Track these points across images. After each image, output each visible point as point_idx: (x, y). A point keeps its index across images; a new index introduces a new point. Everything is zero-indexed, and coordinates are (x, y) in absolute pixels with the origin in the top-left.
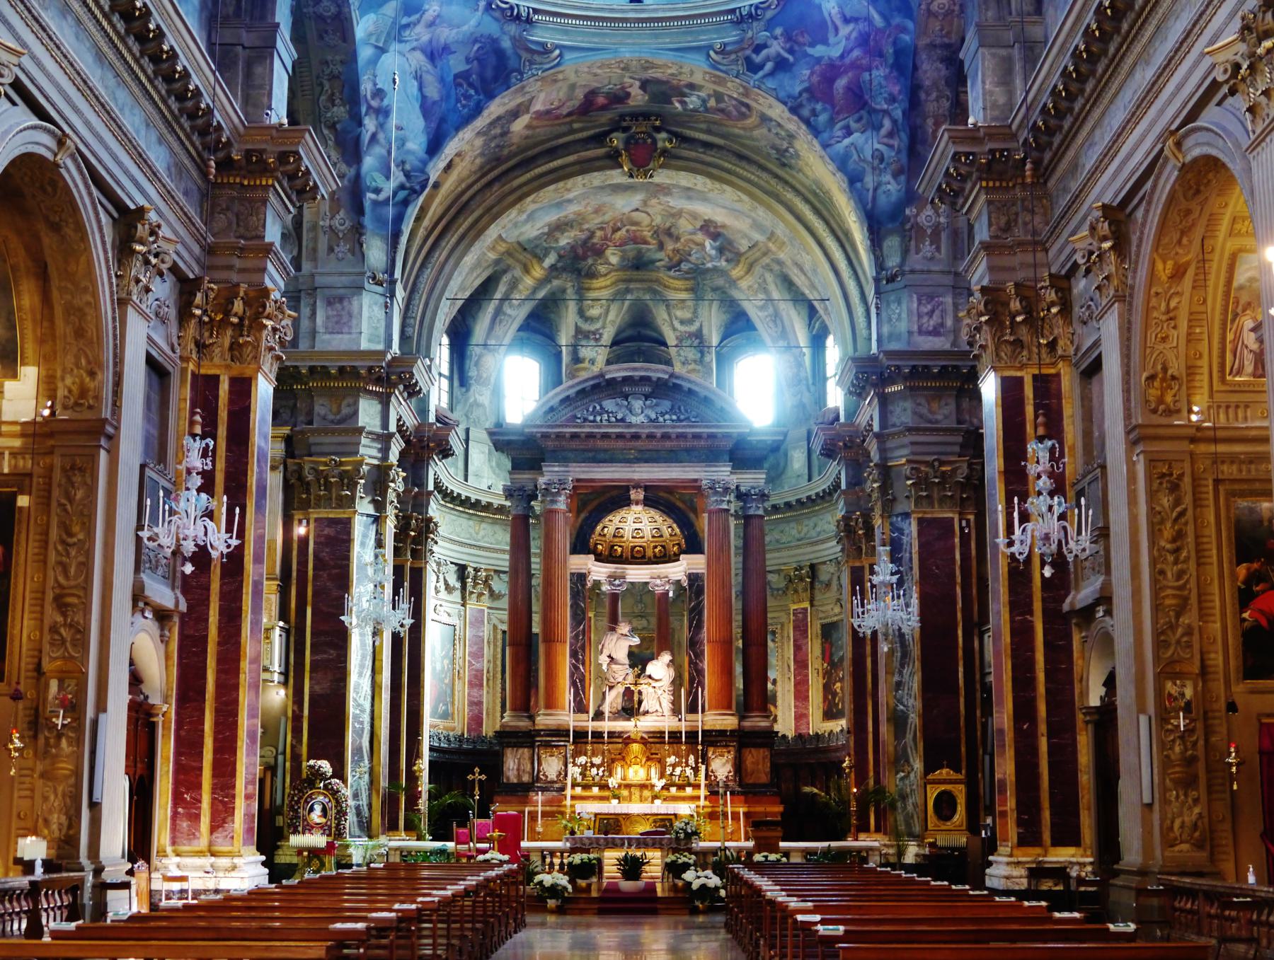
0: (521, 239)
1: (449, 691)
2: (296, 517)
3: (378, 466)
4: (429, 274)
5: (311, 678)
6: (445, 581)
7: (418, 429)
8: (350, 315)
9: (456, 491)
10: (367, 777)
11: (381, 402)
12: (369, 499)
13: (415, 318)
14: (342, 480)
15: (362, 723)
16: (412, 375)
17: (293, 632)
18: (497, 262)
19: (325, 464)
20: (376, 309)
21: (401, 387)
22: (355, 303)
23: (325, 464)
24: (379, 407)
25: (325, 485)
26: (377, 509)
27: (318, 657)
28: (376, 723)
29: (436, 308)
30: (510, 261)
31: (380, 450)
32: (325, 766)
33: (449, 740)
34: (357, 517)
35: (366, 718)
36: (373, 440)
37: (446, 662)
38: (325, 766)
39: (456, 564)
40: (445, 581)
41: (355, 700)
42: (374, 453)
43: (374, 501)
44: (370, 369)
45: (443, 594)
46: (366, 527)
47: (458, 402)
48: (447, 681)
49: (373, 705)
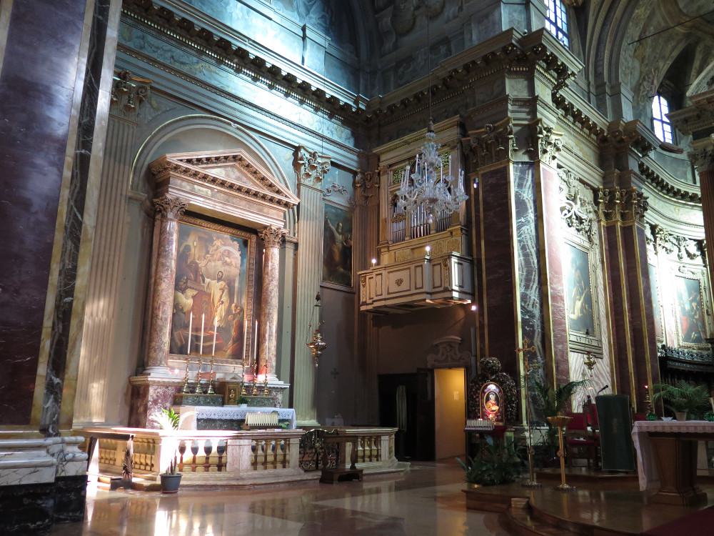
0: (702, 12)
1: (699, 324)
2: (473, 178)
3: (528, 125)
4: (611, 27)
5: (487, 295)
6: (687, 252)
7: (612, 127)
8: (494, 24)
9: (683, 189)
10: (541, 371)
11: (526, 80)
12: (524, 151)
13: (603, 60)
14: (497, 140)
15: (532, 326)
16: (544, 48)
17: (476, 261)
18: (688, 36)
19: (486, 133)
20: (515, 15)
21: (544, 65)
22: (496, 14)
23: (486, 133)
24: (526, 83)
25: (487, 148)
26: (531, 158)
27: (491, 277)
28: (546, 325)
29: (619, 50)
30: (699, 34)
31: (528, 113)
32: (494, 361)
33: (692, 356)
34: (511, 166)
35: (536, 322)
36: (521, 106)
37: (694, 304)
38: (494, 361)
39: (695, 240)
40: (687, 252)
41: (522, 307)
42: (524, 115)
43: (527, 152)
44: (505, 49)
45: (686, 259)
46: (523, 172)
47: (681, 139)
48: (697, 317)
49: (541, 311)
